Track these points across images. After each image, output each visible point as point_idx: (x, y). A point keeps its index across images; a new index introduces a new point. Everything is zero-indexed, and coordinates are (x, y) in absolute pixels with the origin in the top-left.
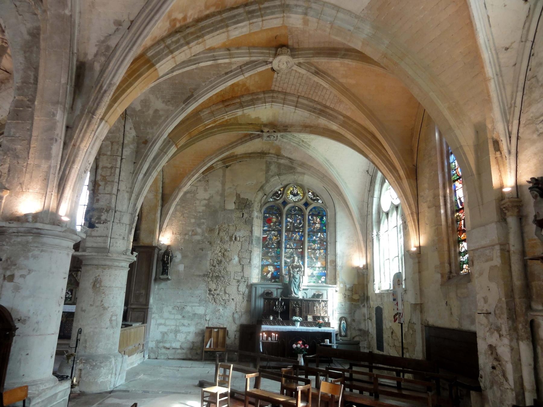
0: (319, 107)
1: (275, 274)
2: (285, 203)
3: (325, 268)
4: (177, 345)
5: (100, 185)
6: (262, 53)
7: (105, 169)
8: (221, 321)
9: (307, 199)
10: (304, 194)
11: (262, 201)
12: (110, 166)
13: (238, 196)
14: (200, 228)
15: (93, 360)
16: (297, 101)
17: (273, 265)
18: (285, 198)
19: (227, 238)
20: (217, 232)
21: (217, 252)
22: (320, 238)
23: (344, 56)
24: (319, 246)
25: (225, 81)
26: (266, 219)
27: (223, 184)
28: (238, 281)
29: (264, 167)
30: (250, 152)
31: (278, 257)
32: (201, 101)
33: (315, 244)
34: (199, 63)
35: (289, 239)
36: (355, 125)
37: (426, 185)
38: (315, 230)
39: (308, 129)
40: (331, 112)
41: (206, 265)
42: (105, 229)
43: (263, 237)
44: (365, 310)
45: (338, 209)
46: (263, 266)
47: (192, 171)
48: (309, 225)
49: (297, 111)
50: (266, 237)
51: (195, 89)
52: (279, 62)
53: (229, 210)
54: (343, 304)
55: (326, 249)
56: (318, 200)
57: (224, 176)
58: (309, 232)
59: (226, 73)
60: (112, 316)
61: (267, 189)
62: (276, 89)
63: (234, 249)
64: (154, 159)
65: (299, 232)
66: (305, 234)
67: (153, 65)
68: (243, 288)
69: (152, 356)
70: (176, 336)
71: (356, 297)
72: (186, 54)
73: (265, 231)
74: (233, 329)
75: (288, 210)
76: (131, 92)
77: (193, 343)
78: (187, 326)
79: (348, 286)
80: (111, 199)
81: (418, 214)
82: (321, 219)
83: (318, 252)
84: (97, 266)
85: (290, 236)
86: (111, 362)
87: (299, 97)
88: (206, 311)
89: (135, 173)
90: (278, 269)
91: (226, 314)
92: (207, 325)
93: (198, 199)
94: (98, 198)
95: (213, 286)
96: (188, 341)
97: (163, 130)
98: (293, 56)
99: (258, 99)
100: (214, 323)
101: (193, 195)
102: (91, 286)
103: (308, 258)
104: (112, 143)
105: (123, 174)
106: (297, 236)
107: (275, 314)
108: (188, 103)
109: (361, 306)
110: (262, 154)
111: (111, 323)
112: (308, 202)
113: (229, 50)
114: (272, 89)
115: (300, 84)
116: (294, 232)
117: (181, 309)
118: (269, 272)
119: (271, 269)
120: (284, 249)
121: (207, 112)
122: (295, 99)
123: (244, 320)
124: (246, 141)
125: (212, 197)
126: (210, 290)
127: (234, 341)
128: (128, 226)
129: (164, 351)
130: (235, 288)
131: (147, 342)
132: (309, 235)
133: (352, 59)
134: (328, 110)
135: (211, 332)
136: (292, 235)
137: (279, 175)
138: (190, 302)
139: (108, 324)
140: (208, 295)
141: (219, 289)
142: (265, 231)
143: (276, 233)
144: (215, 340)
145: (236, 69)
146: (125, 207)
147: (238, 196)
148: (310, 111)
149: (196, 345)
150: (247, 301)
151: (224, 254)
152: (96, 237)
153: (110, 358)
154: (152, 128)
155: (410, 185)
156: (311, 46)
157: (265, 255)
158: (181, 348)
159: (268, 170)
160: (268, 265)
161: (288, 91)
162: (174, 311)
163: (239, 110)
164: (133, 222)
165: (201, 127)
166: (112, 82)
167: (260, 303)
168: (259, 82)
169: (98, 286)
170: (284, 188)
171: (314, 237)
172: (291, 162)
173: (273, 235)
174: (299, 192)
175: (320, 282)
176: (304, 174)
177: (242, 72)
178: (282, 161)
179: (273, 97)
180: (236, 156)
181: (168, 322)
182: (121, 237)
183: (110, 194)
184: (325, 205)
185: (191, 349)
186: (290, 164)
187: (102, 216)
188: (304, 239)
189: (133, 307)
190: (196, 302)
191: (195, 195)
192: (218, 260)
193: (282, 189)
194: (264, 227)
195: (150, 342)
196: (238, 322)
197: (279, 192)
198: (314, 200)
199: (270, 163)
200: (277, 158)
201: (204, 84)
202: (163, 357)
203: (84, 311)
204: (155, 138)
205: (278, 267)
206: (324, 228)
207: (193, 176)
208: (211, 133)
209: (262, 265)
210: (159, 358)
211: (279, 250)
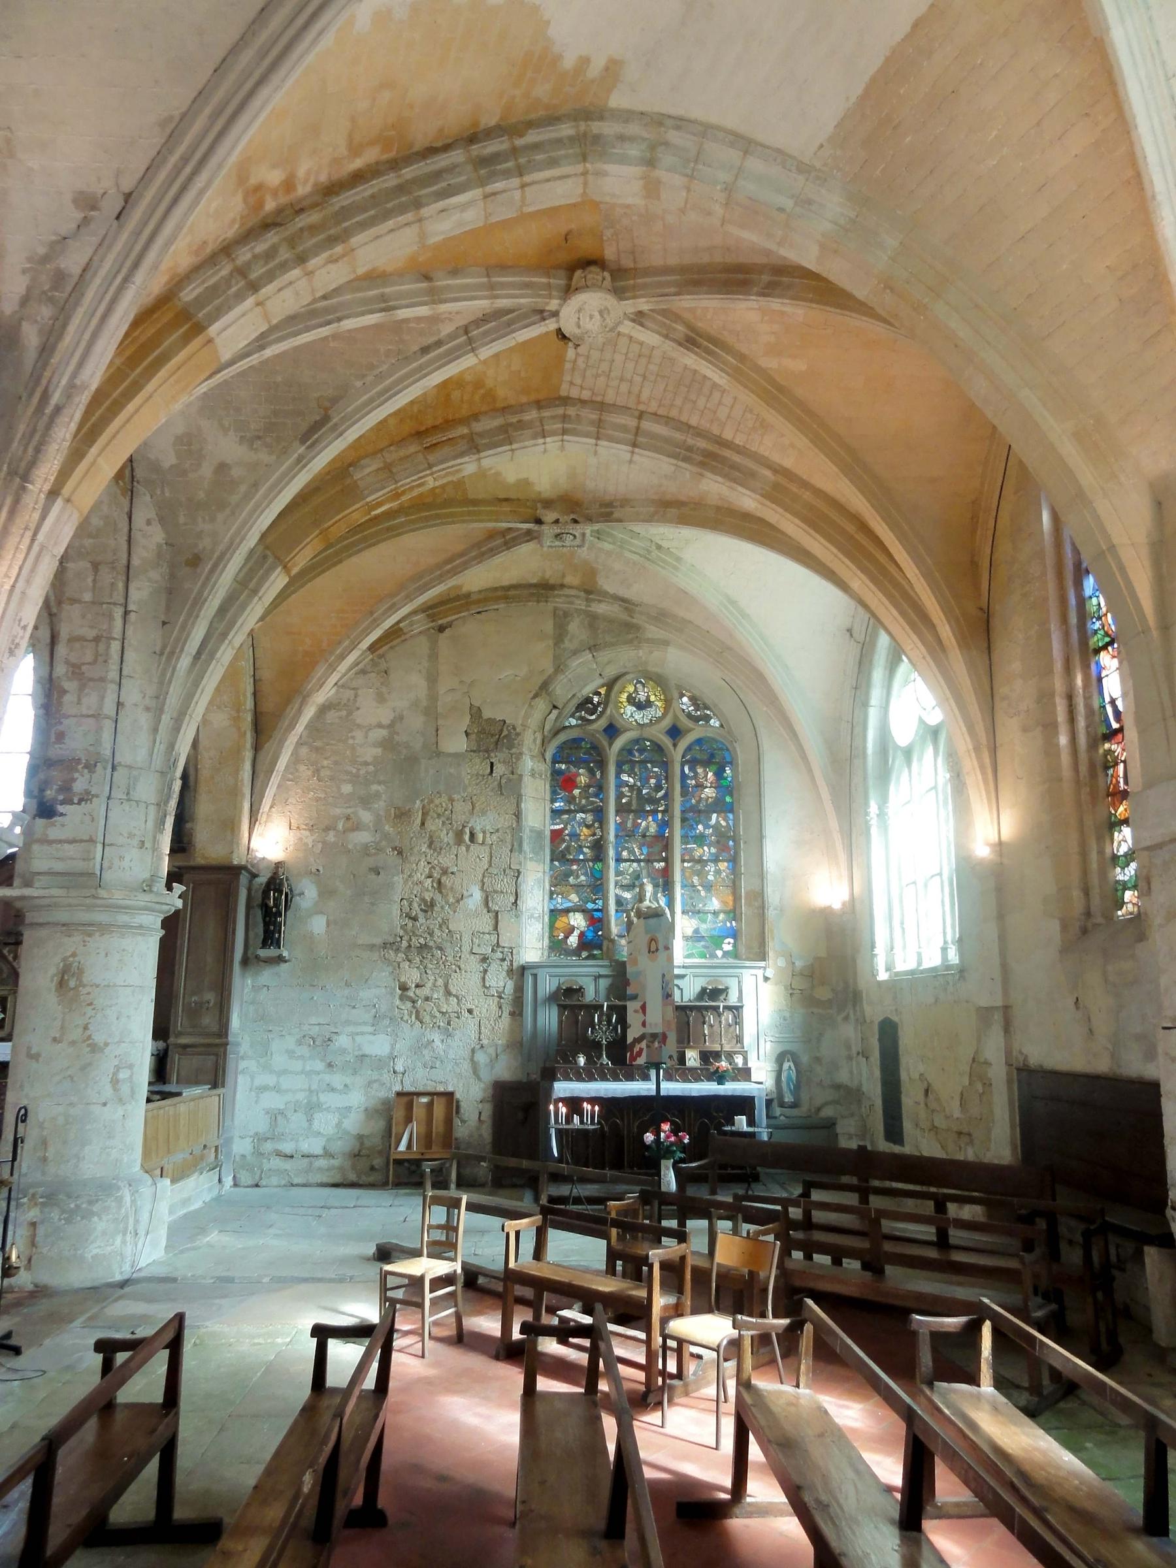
0: (702, 444)
1: (590, 935)
2: (612, 731)
3: (734, 913)
4: (314, 1146)
5: (65, 692)
6: (527, 285)
7: (77, 645)
8: (438, 1074)
9: (675, 716)
10: (668, 703)
11: (547, 727)
12: (91, 634)
13: (476, 713)
14: (369, 809)
15: (69, 1197)
16: (638, 428)
17: (584, 911)
18: (611, 716)
19: (447, 837)
20: (418, 821)
21: (418, 876)
22: (717, 827)
23: (769, 290)
24: (713, 850)
25: (421, 372)
26: (561, 778)
27: (432, 679)
28: (484, 959)
29: (549, 626)
30: (506, 583)
31: (598, 886)
32: (353, 434)
33: (701, 846)
34: (339, 320)
35: (626, 834)
36: (807, 495)
37: (1016, 666)
38: (702, 806)
39: (673, 511)
40: (737, 458)
41: (391, 916)
42: (87, 819)
43: (553, 832)
44: (849, 1031)
45: (766, 743)
46: (555, 913)
47: (340, 643)
48: (685, 792)
49: (636, 458)
50: (561, 831)
51: (334, 401)
52: (579, 311)
53: (450, 755)
54: (787, 1015)
55: (734, 860)
56: (707, 718)
57: (433, 656)
58: (683, 812)
59: (425, 350)
60: (118, 1068)
61: (558, 691)
62: (574, 393)
63: (467, 867)
64: (222, 610)
65: (654, 812)
66: (672, 817)
67: (199, 328)
68: (499, 979)
69: (245, 1178)
70: (310, 1121)
71: (823, 994)
72: (297, 294)
73: (556, 813)
74: (473, 1095)
75: (622, 750)
76: (137, 411)
77: (360, 1138)
78: (340, 1092)
79: (799, 964)
80: (99, 730)
81: (994, 750)
82: (719, 774)
83: (711, 867)
84: (67, 928)
85: (629, 824)
86: (120, 1200)
87: (641, 416)
88: (393, 1047)
89: (167, 654)
90: (597, 921)
91: (451, 1056)
92: (398, 1088)
93: (359, 726)
94: (61, 728)
95: (412, 975)
96: (347, 1133)
97: (245, 523)
98: (619, 293)
99: (521, 425)
100: (419, 1079)
101: (344, 713)
102: (53, 986)
103: (683, 887)
104: (96, 566)
105: (130, 655)
106: (649, 825)
107: (591, 1049)
108: (316, 441)
109: (839, 1018)
110: (543, 589)
111: (115, 1090)
112: (679, 725)
113: (427, 278)
114: (563, 393)
115: (644, 377)
116: (641, 813)
117: (322, 1044)
118: (572, 930)
119: (578, 921)
120: (612, 864)
121: (372, 466)
122: (632, 423)
123: (505, 1069)
124: (493, 552)
125: (401, 718)
126: (404, 988)
127: (478, 1129)
128: (152, 810)
129: (276, 1163)
130: (476, 978)
131: (229, 1141)
132: (683, 820)
133: (792, 298)
134: (727, 453)
135: (409, 1107)
136: (634, 821)
137: (594, 648)
138: (348, 1022)
139: (108, 1092)
140: (398, 1002)
141: (429, 984)
142: (556, 813)
143: (589, 818)
144: (423, 1130)
145: (452, 336)
146: (141, 756)
147: (476, 713)
148: (675, 456)
149: (367, 1143)
150: (512, 1014)
151: (439, 882)
152: (60, 842)
153: (119, 1188)
154: (213, 520)
155: (971, 665)
156: (673, 261)
157: (559, 882)
158: (327, 1154)
159: (560, 635)
160: (567, 911)
161: (610, 397)
162: (304, 1051)
163: (467, 459)
164: (169, 797)
165: (355, 514)
166: (78, 382)
167: (549, 1020)
168: (523, 374)
169: (72, 984)
170: (610, 685)
171: (700, 827)
172: (626, 608)
173: (580, 824)
174: (652, 698)
175: (719, 953)
176: (666, 643)
177: (471, 346)
178: (601, 608)
179: (565, 418)
180: (468, 595)
181: (286, 1083)
182: (135, 842)
183: (96, 716)
184: (730, 732)
185: (356, 1155)
186: (624, 616)
187: (74, 780)
188: (671, 832)
189: (183, 1040)
190: (365, 1023)
191: (350, 713)
192: (423, 900)
193: (603, 691)
194: (553, 801)
195: (236, 1140)
196: (488, 1076)
197: (596, 699)
198: (696, 719)
199: (566, 614)
200: (587, 600)
201: (359, 384)
202: (274, 1180)
203: (36, 1057)
204: (221, 547)
205: (597, 915)
206: (728, 799)
207: (342, 657)
208: (388, 529)
209: (552, 911)
210: (263, 1183)
211: (599, 866)
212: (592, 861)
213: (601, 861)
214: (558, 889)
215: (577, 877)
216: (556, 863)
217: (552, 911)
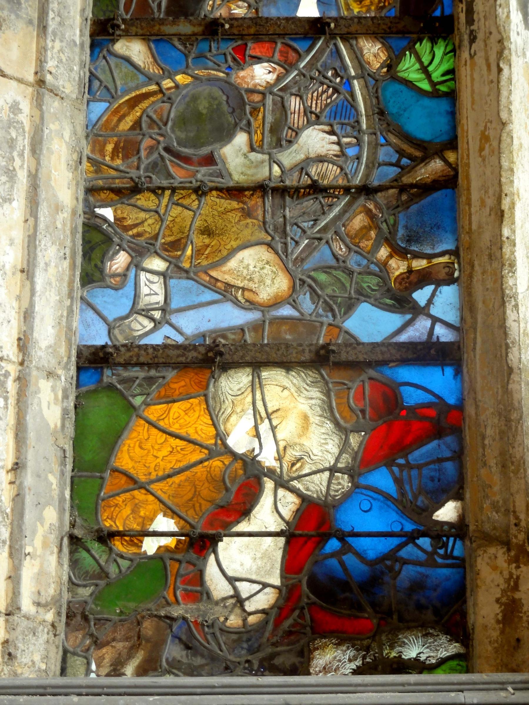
1: (371, 523)
17: (328, 361)
118: (238, 489)
119: (288, 426)
160: (210, 358)
209: (93, 361)
211: (424, 63)
212: (379, 30)
213: (442, 29)
214: (142, 215)
215: (281, 135)
216: (135, 50)
217: (93, 361)
